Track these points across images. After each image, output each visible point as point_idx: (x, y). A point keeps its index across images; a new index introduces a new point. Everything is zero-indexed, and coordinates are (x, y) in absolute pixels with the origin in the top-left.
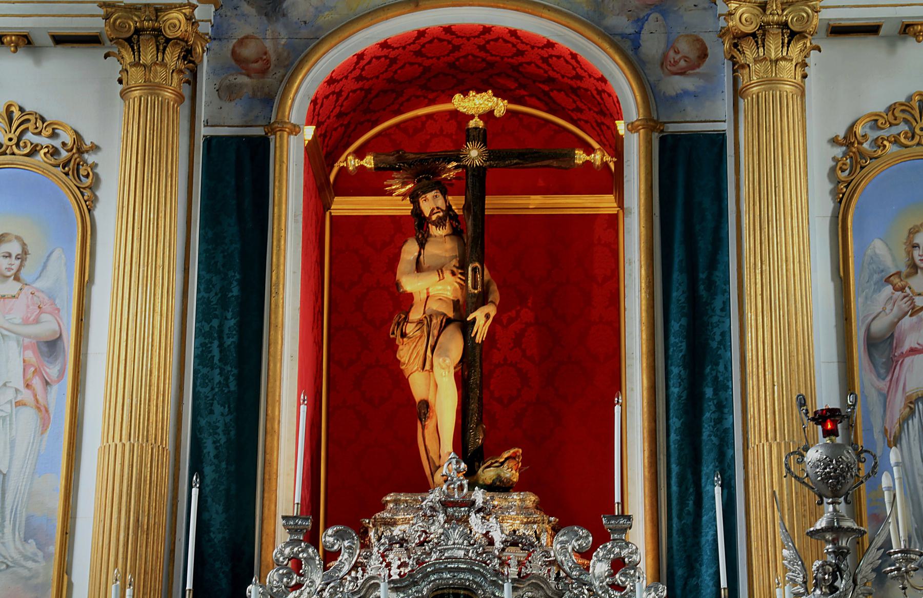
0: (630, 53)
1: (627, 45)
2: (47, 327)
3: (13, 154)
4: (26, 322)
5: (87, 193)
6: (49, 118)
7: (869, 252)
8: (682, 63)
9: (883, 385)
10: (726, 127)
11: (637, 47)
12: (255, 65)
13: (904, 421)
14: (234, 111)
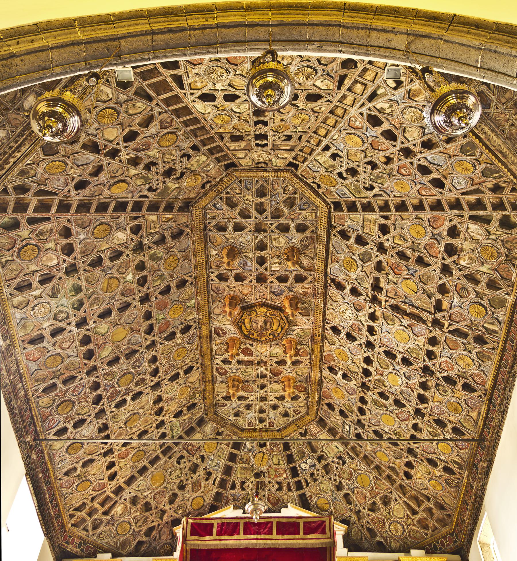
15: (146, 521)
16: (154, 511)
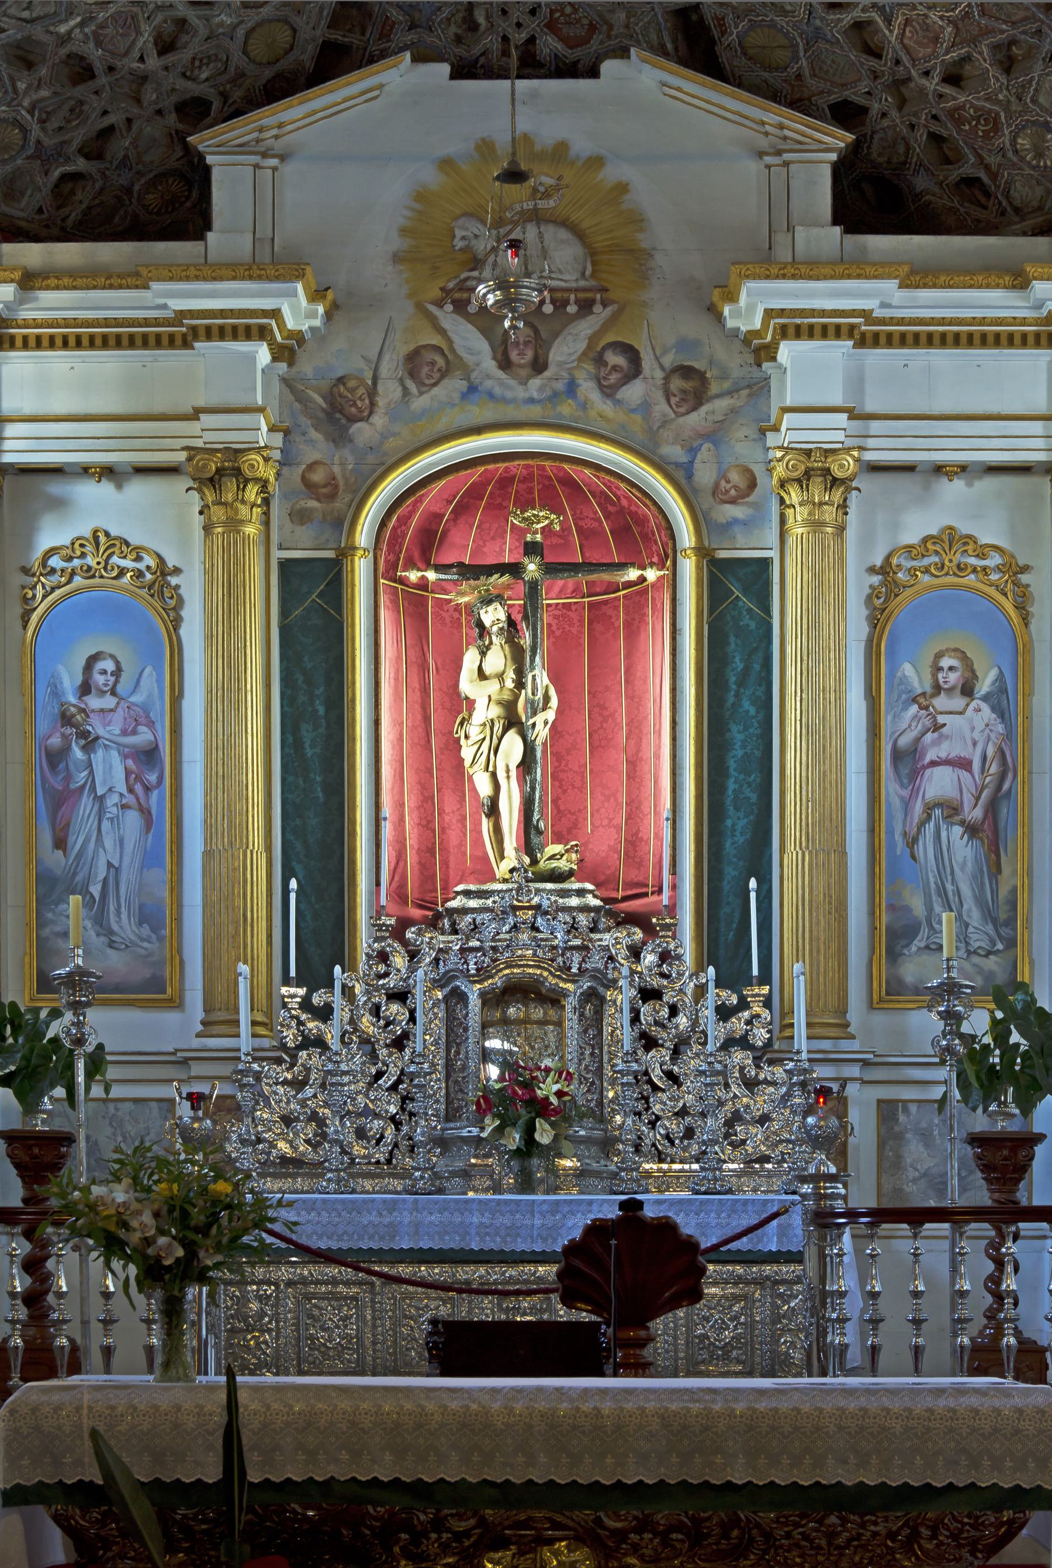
0: (683, 482)
1: (680, 475)
2: (144, 737)
3: (102, 577)
4: (124, 733)
5: (172, 614)
6: (134, 541)
7: (899, 674)
8: (733, 492)
9: (906, 793)
10: (774, 554)
11: (690, 476)
12: (324, 490)
13: (922, 824)
14: (305, 533)
15: (77, 109)
16: (102, 80)
